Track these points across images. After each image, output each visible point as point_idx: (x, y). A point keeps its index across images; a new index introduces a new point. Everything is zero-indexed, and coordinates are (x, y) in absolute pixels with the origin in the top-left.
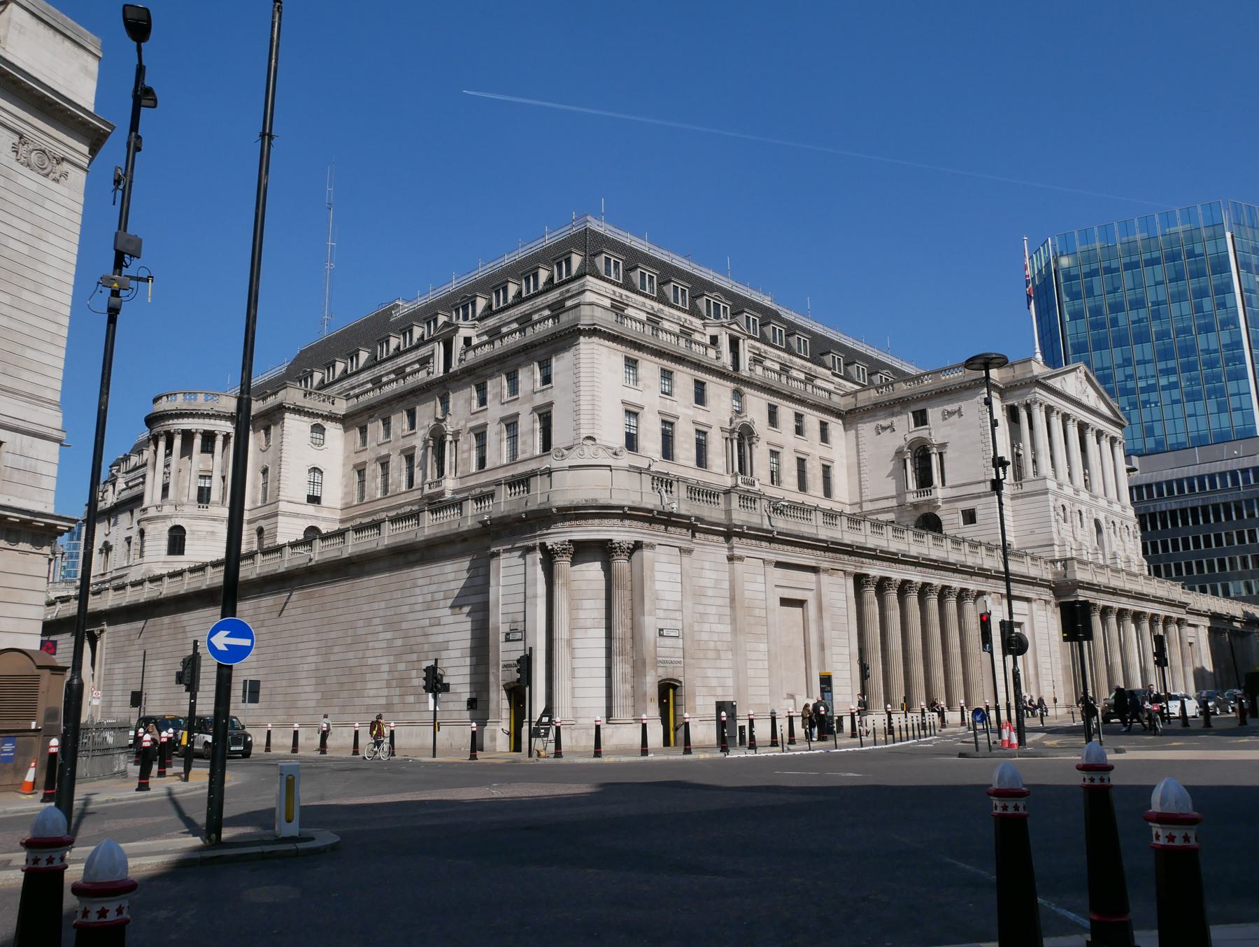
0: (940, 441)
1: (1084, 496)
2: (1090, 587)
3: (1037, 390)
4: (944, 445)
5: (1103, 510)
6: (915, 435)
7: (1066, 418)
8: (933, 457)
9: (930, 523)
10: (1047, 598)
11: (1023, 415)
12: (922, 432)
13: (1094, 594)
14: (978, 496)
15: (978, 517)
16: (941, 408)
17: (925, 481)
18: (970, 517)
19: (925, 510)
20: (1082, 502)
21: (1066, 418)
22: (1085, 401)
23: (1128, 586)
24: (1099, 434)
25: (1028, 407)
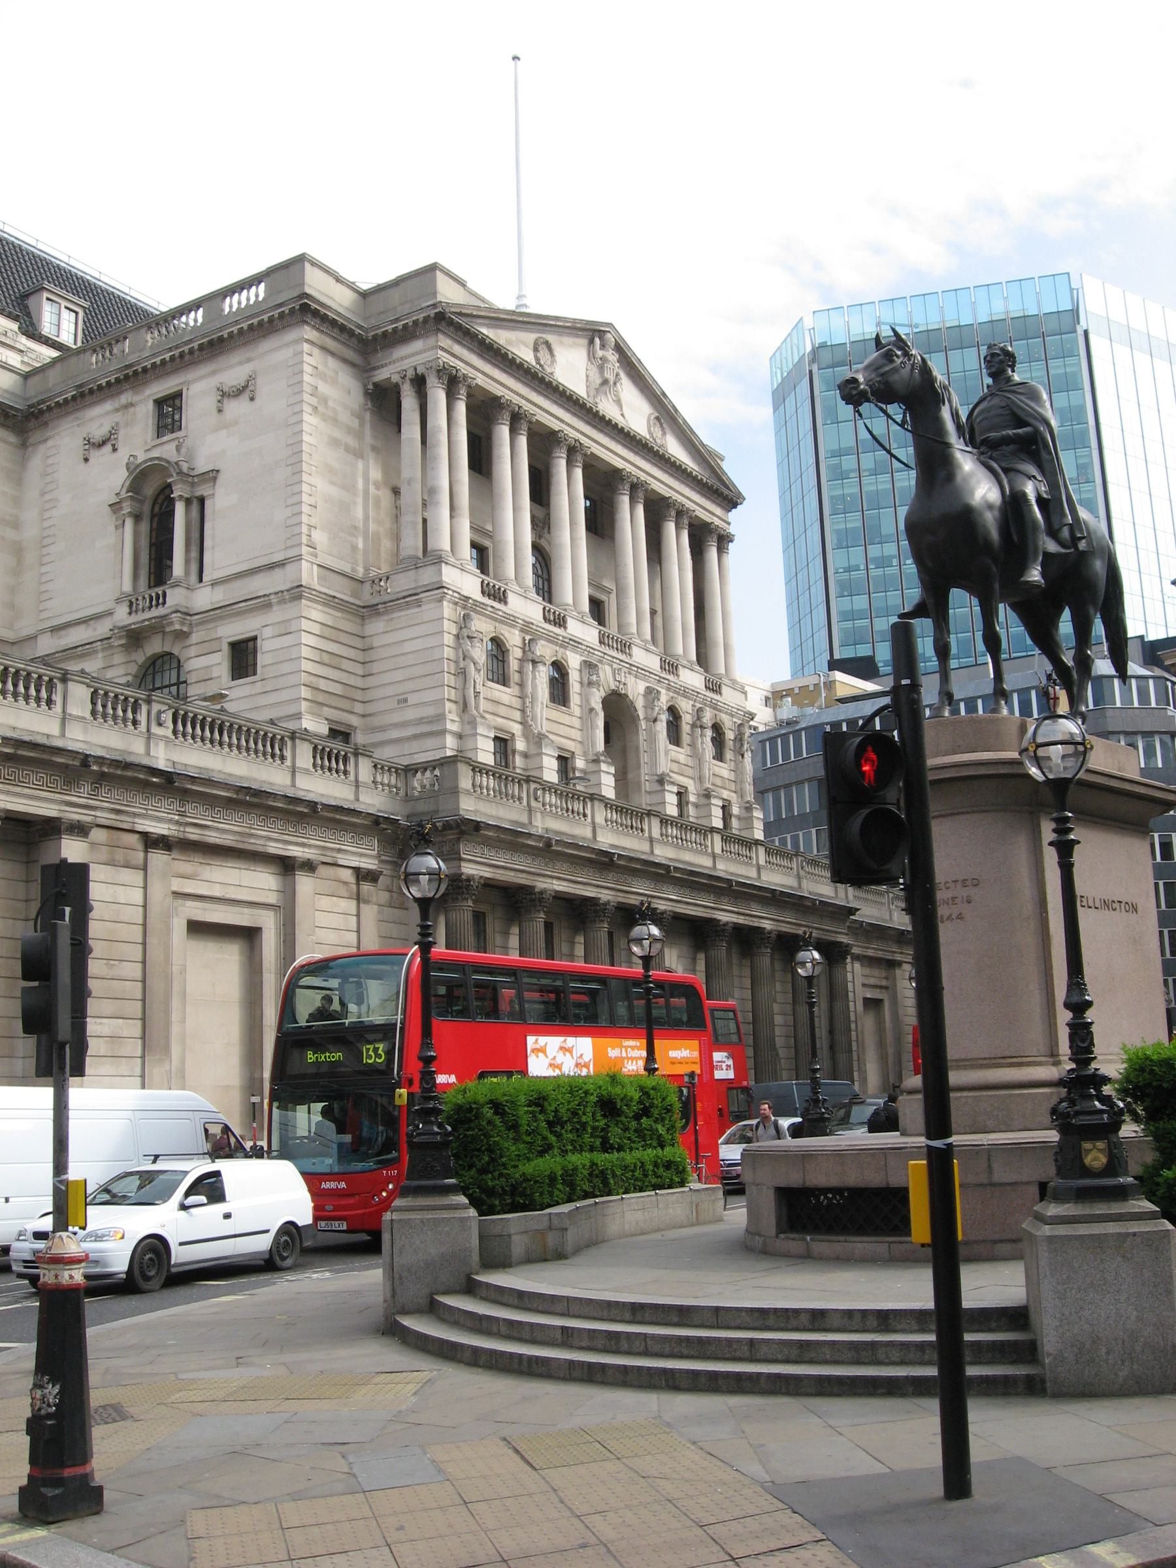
0: (202, 466)
1: (584, 631)
2: (512, 840)
3: (445, 342)
4: (212, 476)
5: (640, 672)
6: (155, 453)
7: (544, 443)
8: (180, 508)
9: (159, 673)
10: (369, 864)
11: (409, 403)
12: (167, 451)
13: (521, 862)
14: (263, 603)
15: (262, 660)
16: (214, 381)
17: (157, 564)
18: (243, 657)
19: (155, 646)
20: (574, 644)
21: (544, 443)
22: (607, 408)
23: (663, 854)
24: (657, 511)
25: (419, 383)
